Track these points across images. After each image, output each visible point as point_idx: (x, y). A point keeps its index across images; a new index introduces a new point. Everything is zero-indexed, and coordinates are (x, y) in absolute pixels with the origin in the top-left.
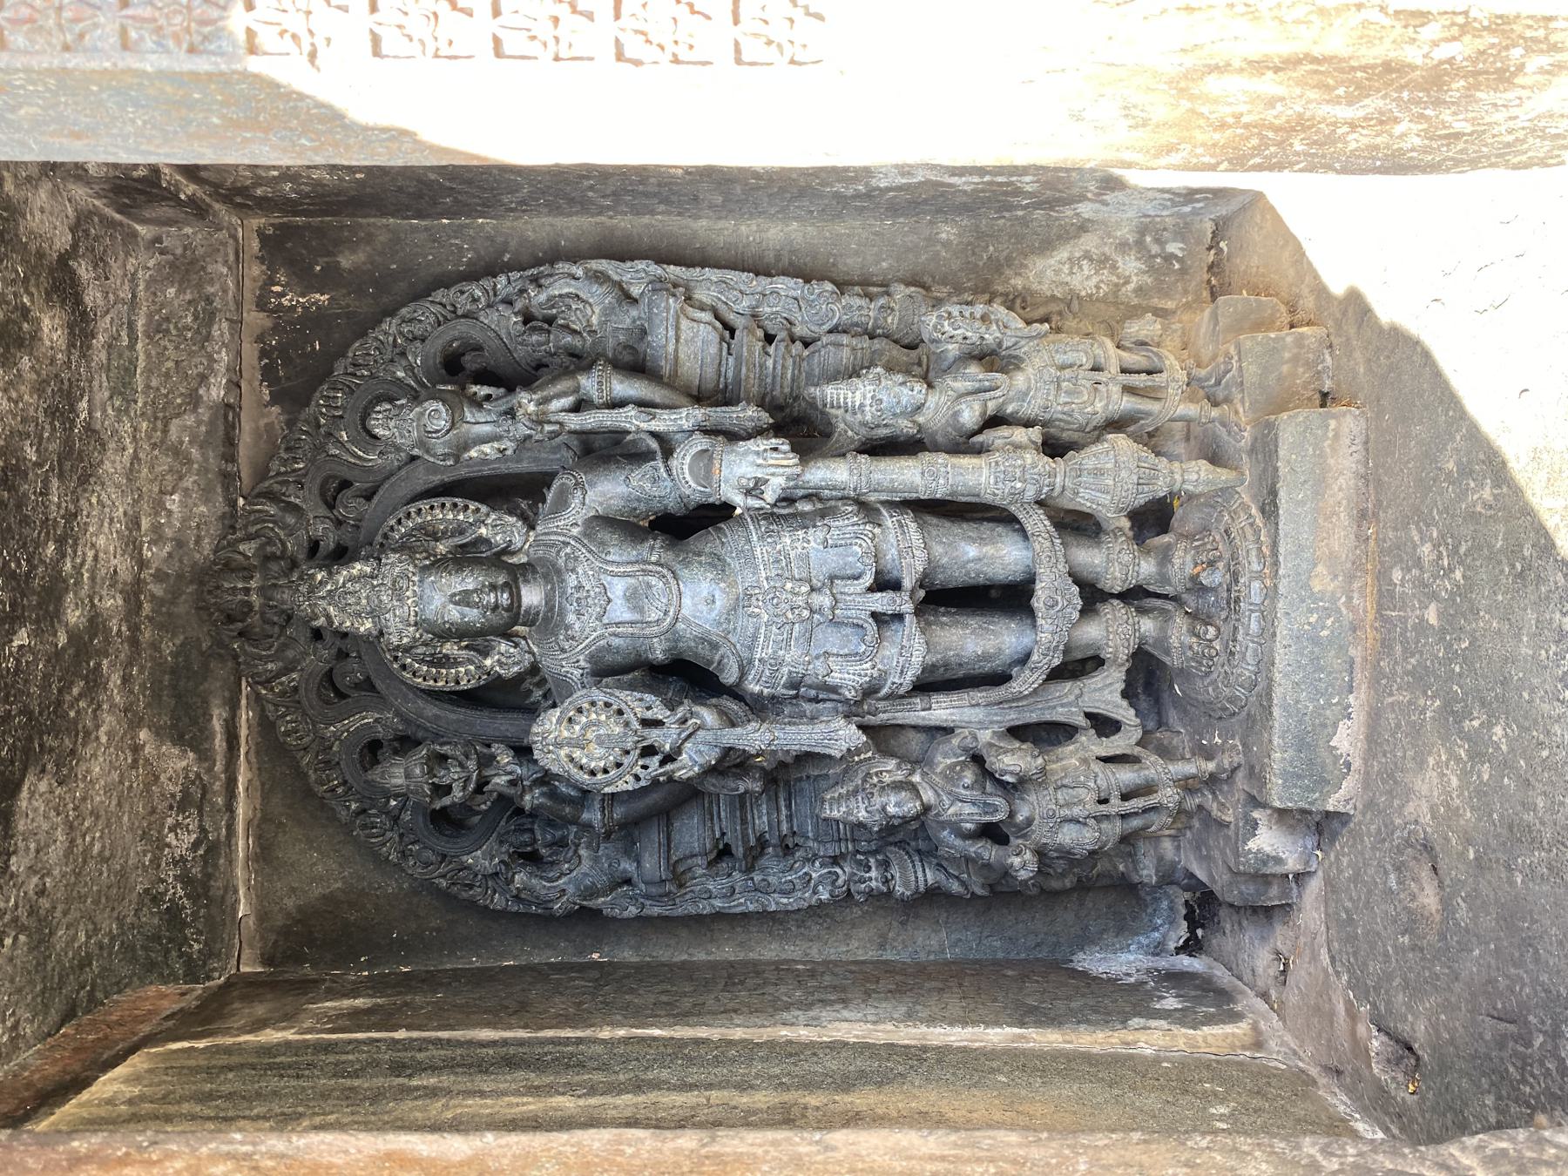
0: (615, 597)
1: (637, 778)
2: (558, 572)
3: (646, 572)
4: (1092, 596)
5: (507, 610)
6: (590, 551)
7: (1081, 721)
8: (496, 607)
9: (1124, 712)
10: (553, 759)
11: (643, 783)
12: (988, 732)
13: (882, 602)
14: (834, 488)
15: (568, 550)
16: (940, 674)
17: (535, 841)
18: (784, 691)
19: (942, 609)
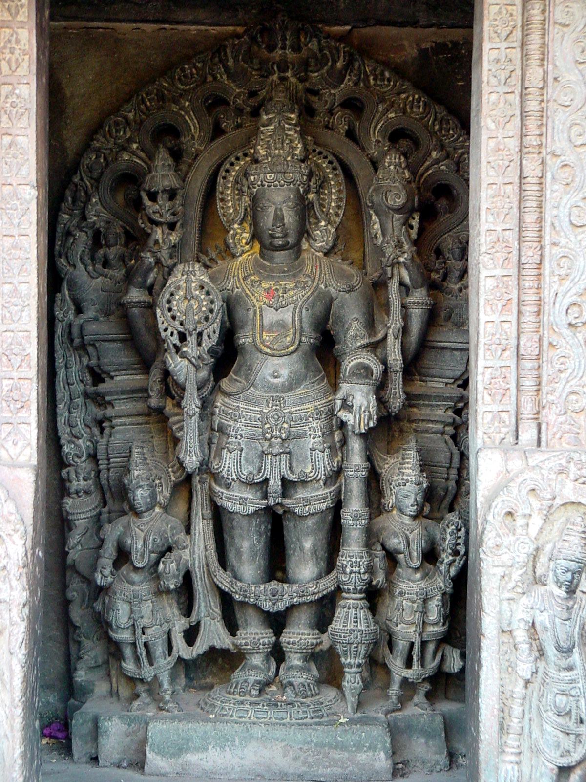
0: (277, 313)
1: (166, 330)
2: (295, 276)
3: (295, 334)
4: (277, 622)
5: (271, 243)
6: (308, 298)
7: (194, 618)
8: (272, 237)
9: (201, 646)
10: (177, 278)
11: (163, 334)
12: (188, 557)
13: (275, 485)
14: (348, 455)
15: (310, 283)
16: (226, 524)
17: (109, 246)
18: (217, 422)
19: (269, 527)
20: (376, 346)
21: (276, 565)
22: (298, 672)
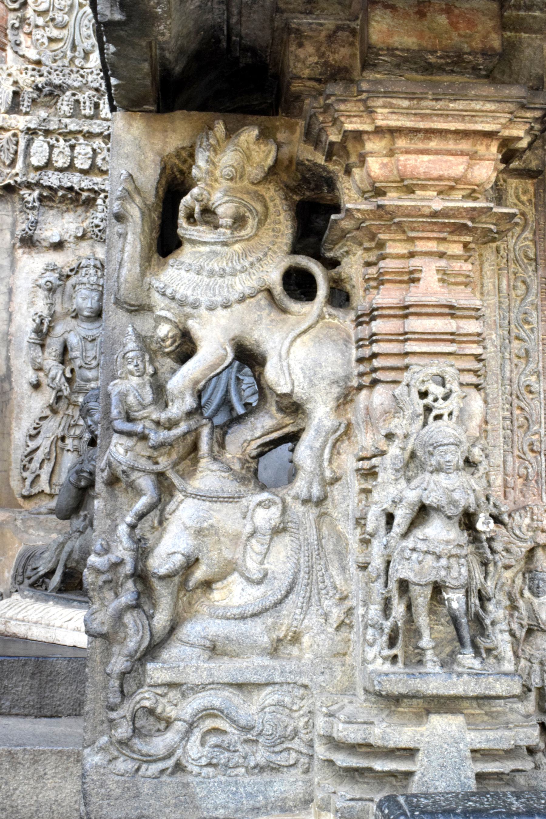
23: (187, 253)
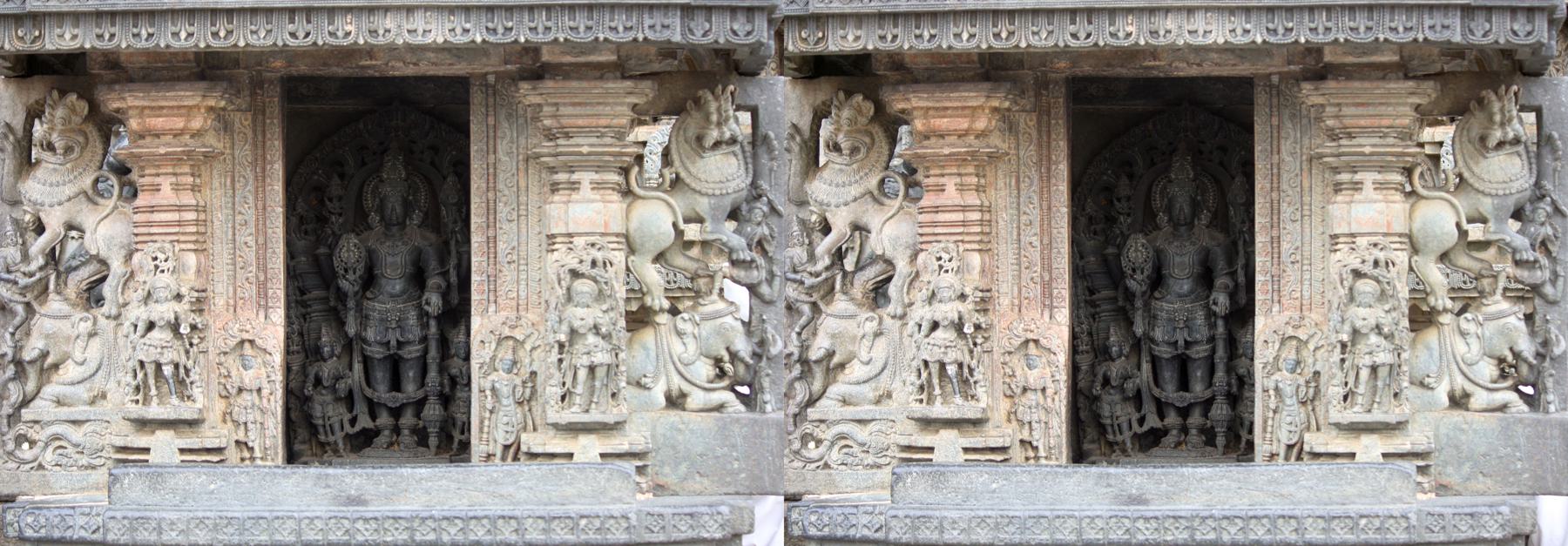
20: (445, 274)
21: (396, 385)
22: (407, 437)
23: (40, 173)
